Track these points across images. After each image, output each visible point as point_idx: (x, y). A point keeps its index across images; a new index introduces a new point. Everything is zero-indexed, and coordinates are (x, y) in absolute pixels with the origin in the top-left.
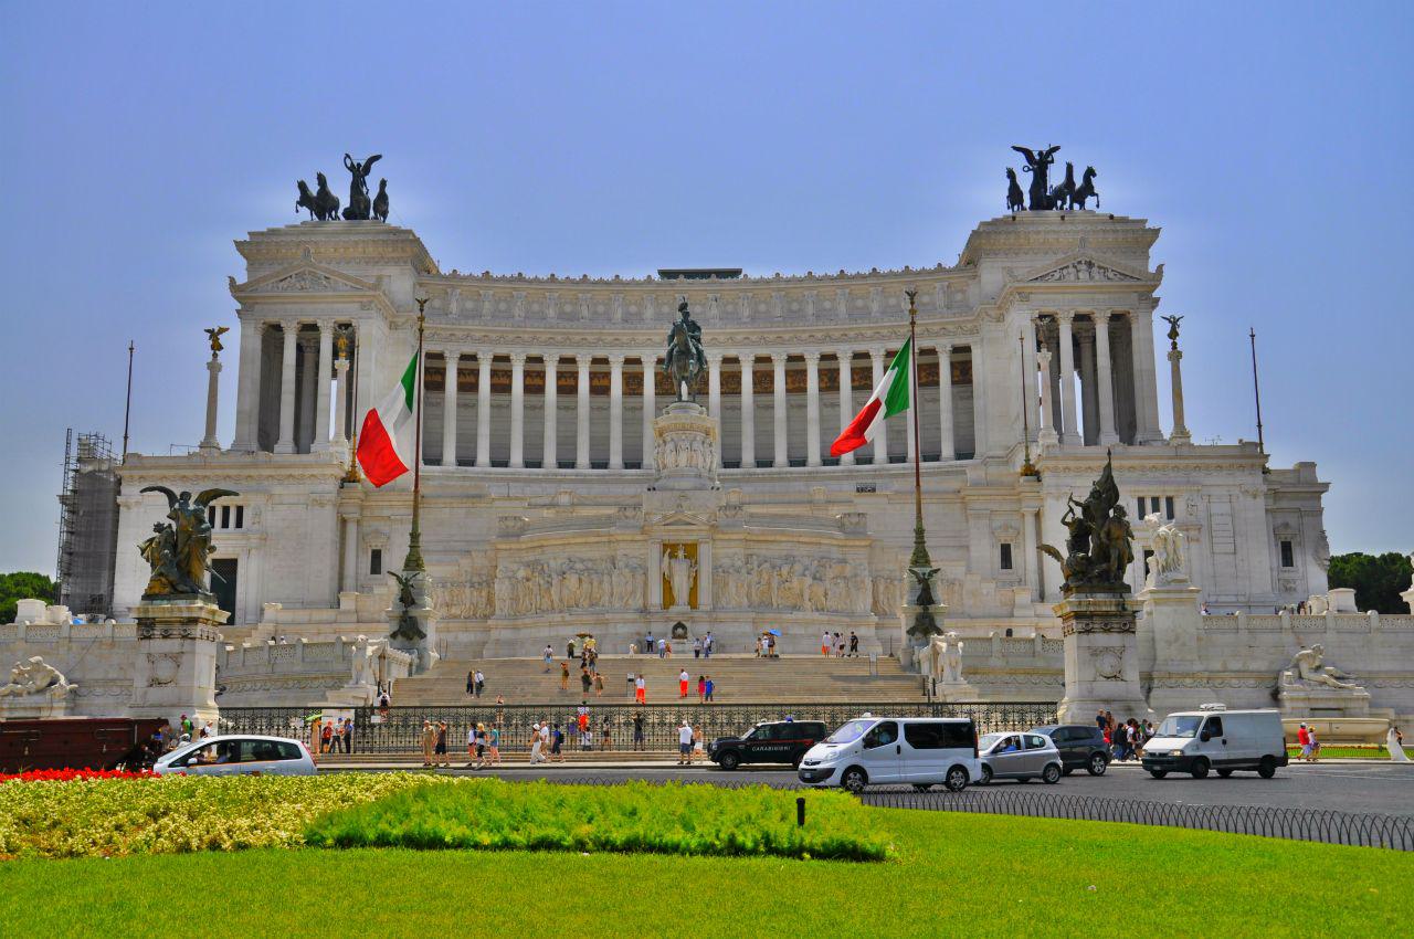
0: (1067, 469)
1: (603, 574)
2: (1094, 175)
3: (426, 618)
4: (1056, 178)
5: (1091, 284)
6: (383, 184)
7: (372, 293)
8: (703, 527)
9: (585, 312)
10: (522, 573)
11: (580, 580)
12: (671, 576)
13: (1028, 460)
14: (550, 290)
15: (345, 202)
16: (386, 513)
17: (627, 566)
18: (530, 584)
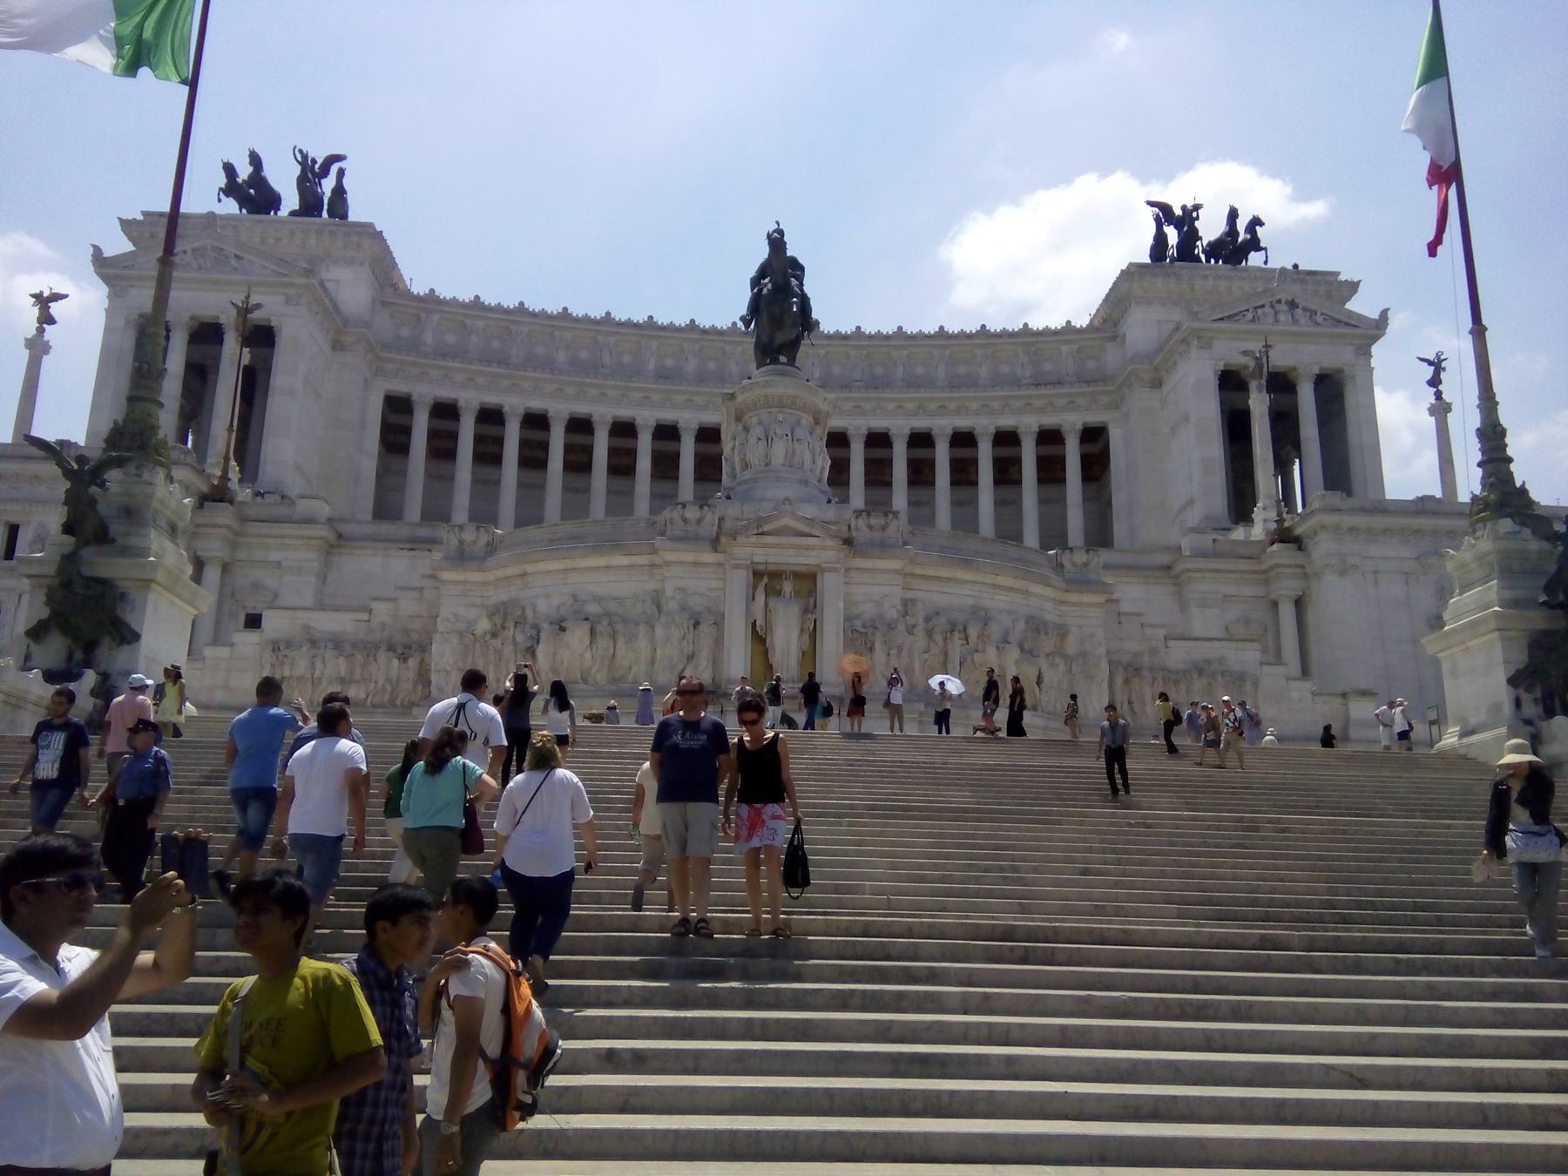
0: (1352, 530)
1: (637, 624)
2: (1261, 224)
3: (147, 583)
4: (1210, 228)
5: (1294, 328)
6: (341, 173)
7: (302, 281)
8: (830, 543)
9: (607, 359)
10: (484, 625)
11: (592, 631)
12: (768, 625)
13: (1280, 521)
14: (561, 328)
15: (290, 201)
16: (275, 556)
17: (683, 608)
18: (497, 642)
